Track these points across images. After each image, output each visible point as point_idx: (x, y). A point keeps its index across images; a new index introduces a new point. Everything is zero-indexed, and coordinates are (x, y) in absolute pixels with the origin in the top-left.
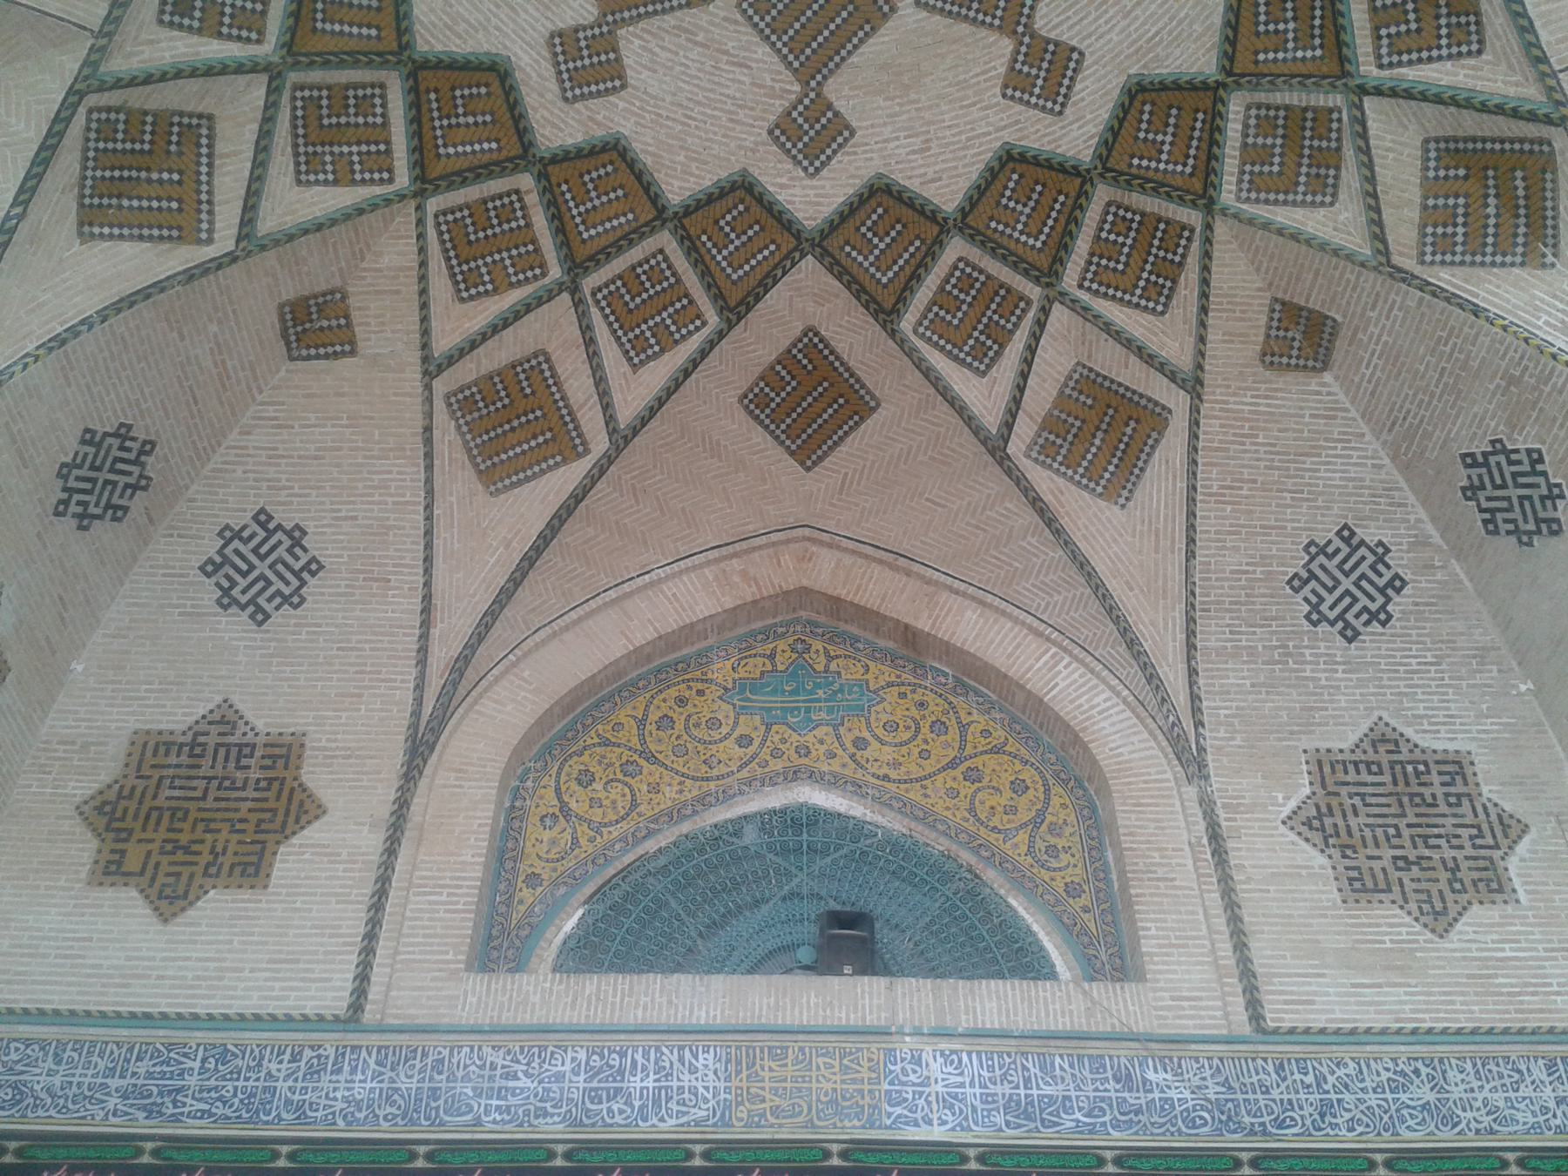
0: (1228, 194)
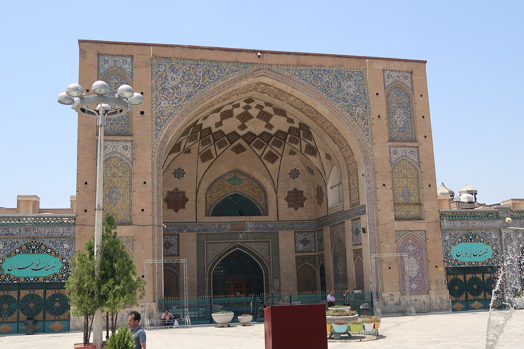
0: (287, 141)
